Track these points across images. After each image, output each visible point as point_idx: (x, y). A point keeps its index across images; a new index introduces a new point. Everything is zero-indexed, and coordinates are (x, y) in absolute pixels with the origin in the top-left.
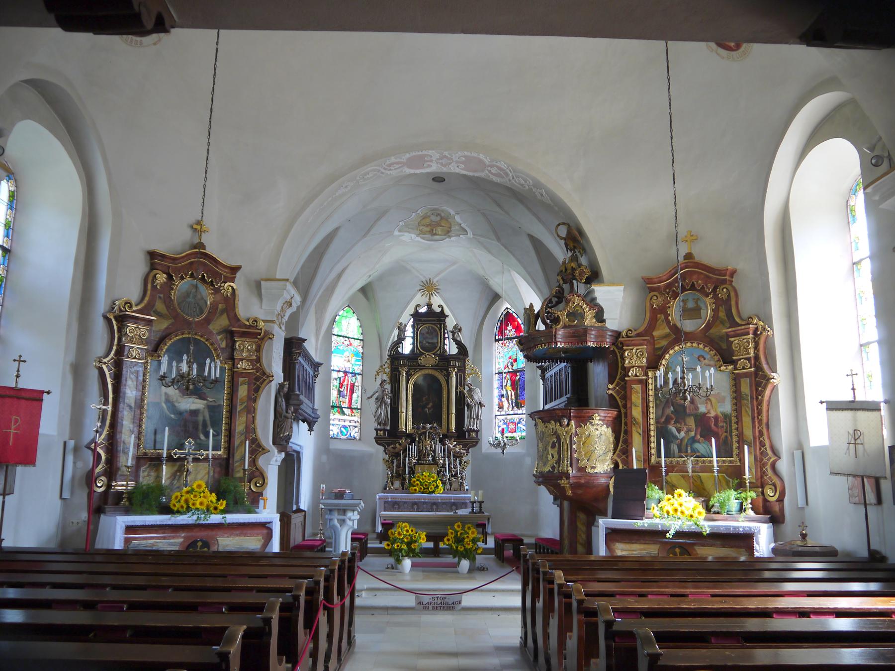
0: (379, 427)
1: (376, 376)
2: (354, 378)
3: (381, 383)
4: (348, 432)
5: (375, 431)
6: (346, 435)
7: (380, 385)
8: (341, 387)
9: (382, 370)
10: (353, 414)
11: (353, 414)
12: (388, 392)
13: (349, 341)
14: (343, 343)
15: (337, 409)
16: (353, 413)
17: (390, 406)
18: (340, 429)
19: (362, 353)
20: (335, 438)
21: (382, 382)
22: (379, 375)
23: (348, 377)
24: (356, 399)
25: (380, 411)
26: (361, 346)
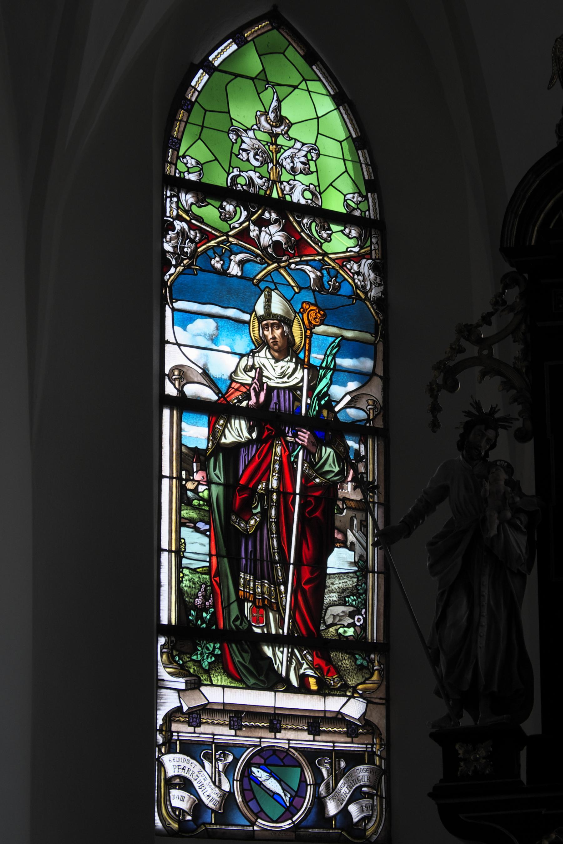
0: (466, 720)
1: (433, 391)
2: (328, 452)
3: (463, 437)
4: (299, 794)
5: (438, 750)
6: (290, 812)
7: (460, 446)
8: (246, 514)
9: (472, 351)
10: (333, 680)
11: (333, 680)
12: (514, 485)
13: (287, 228)
14: (244, 235)
15: (215, 647)
16: (337, 670)
17: (533, 579)
18: (247, 775)
19: (380, 303)
20: (211, 835)
21: (468, 427)
22: (453, 388)
23: (290, 448)
24: (350, 583)
25: (463, 610)
26: (365, 266)
